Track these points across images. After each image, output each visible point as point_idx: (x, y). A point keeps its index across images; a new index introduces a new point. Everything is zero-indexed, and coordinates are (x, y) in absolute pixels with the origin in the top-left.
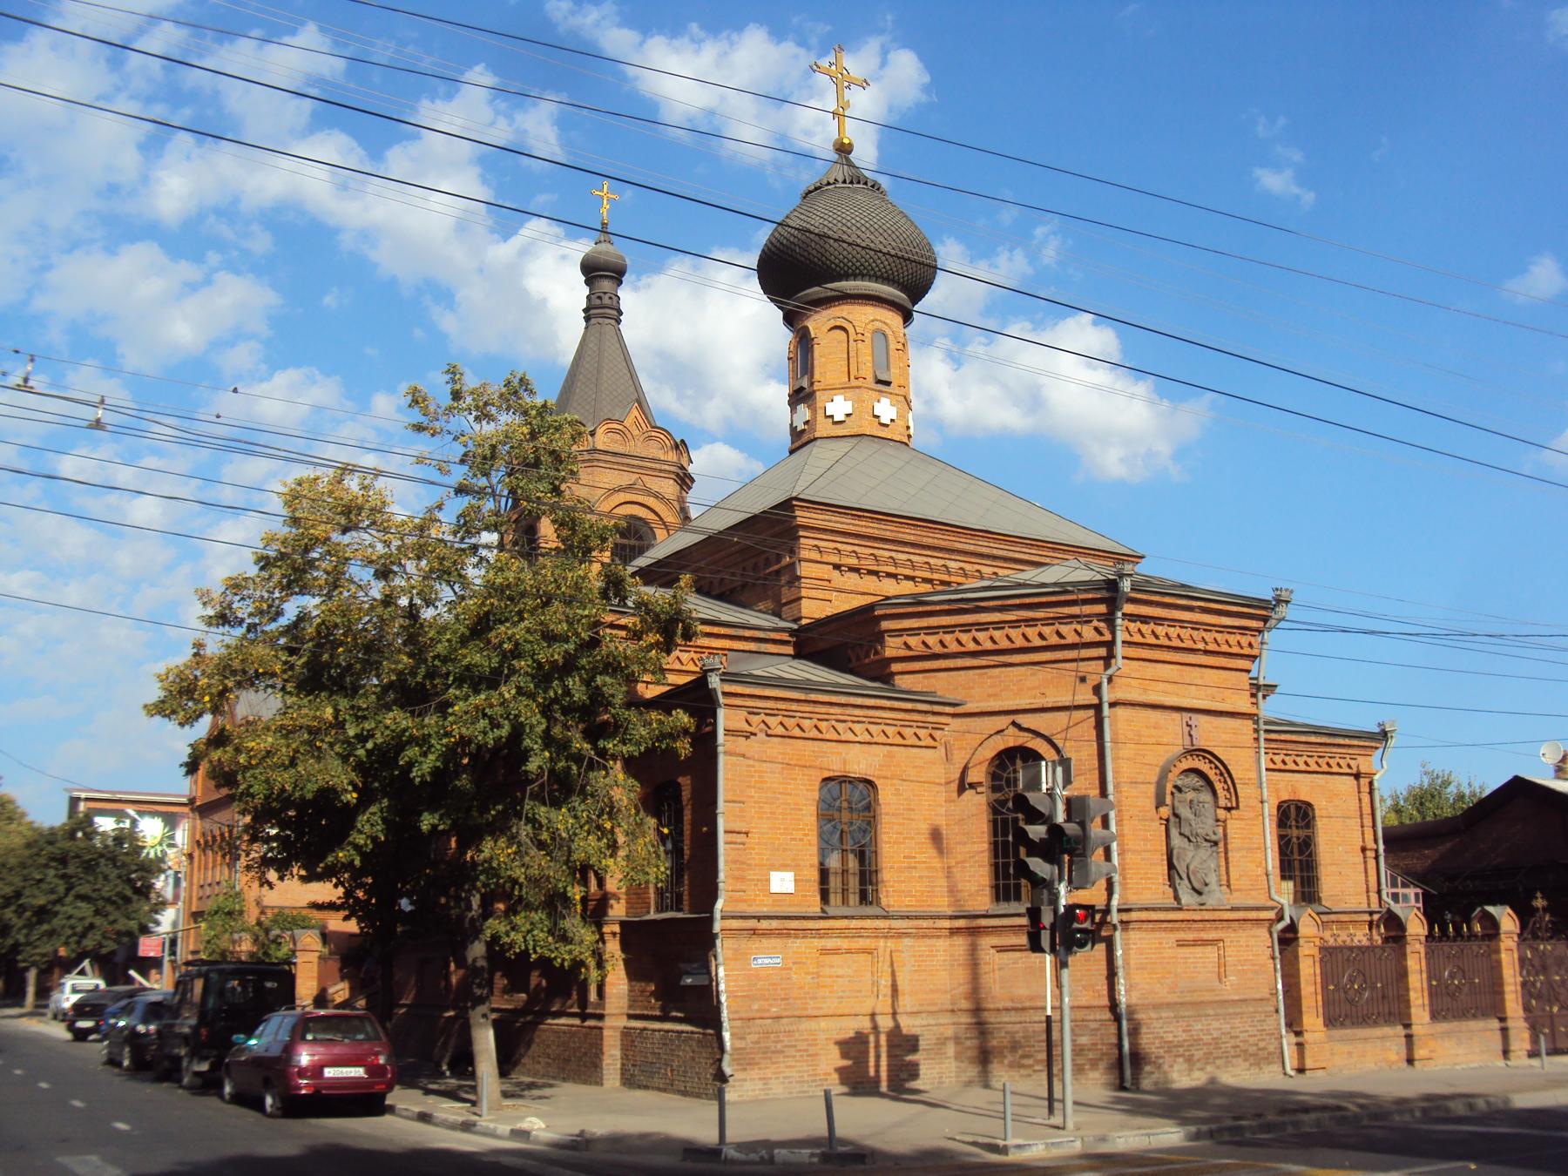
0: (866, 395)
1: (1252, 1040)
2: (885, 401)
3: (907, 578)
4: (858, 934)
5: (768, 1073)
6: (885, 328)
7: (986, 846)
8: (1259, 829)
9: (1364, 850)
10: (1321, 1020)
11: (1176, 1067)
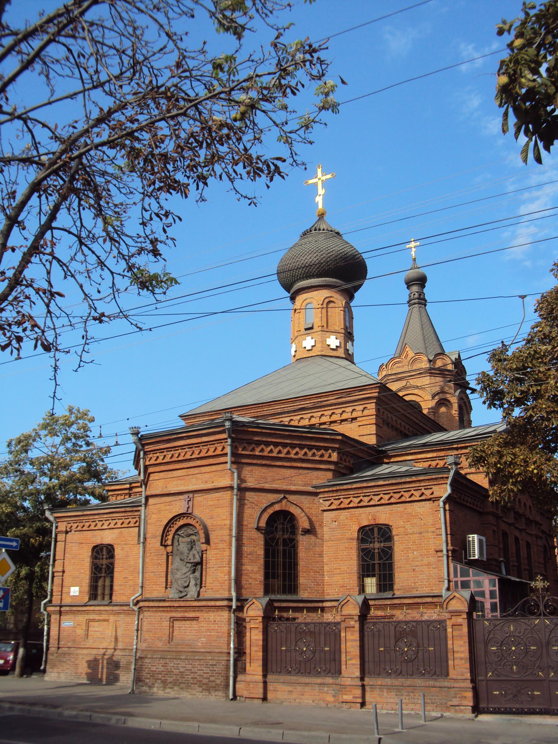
1: (205, 675)
4: (100, 612)
5: (60, 670)
8: (227, 553)
11: (156, 685)
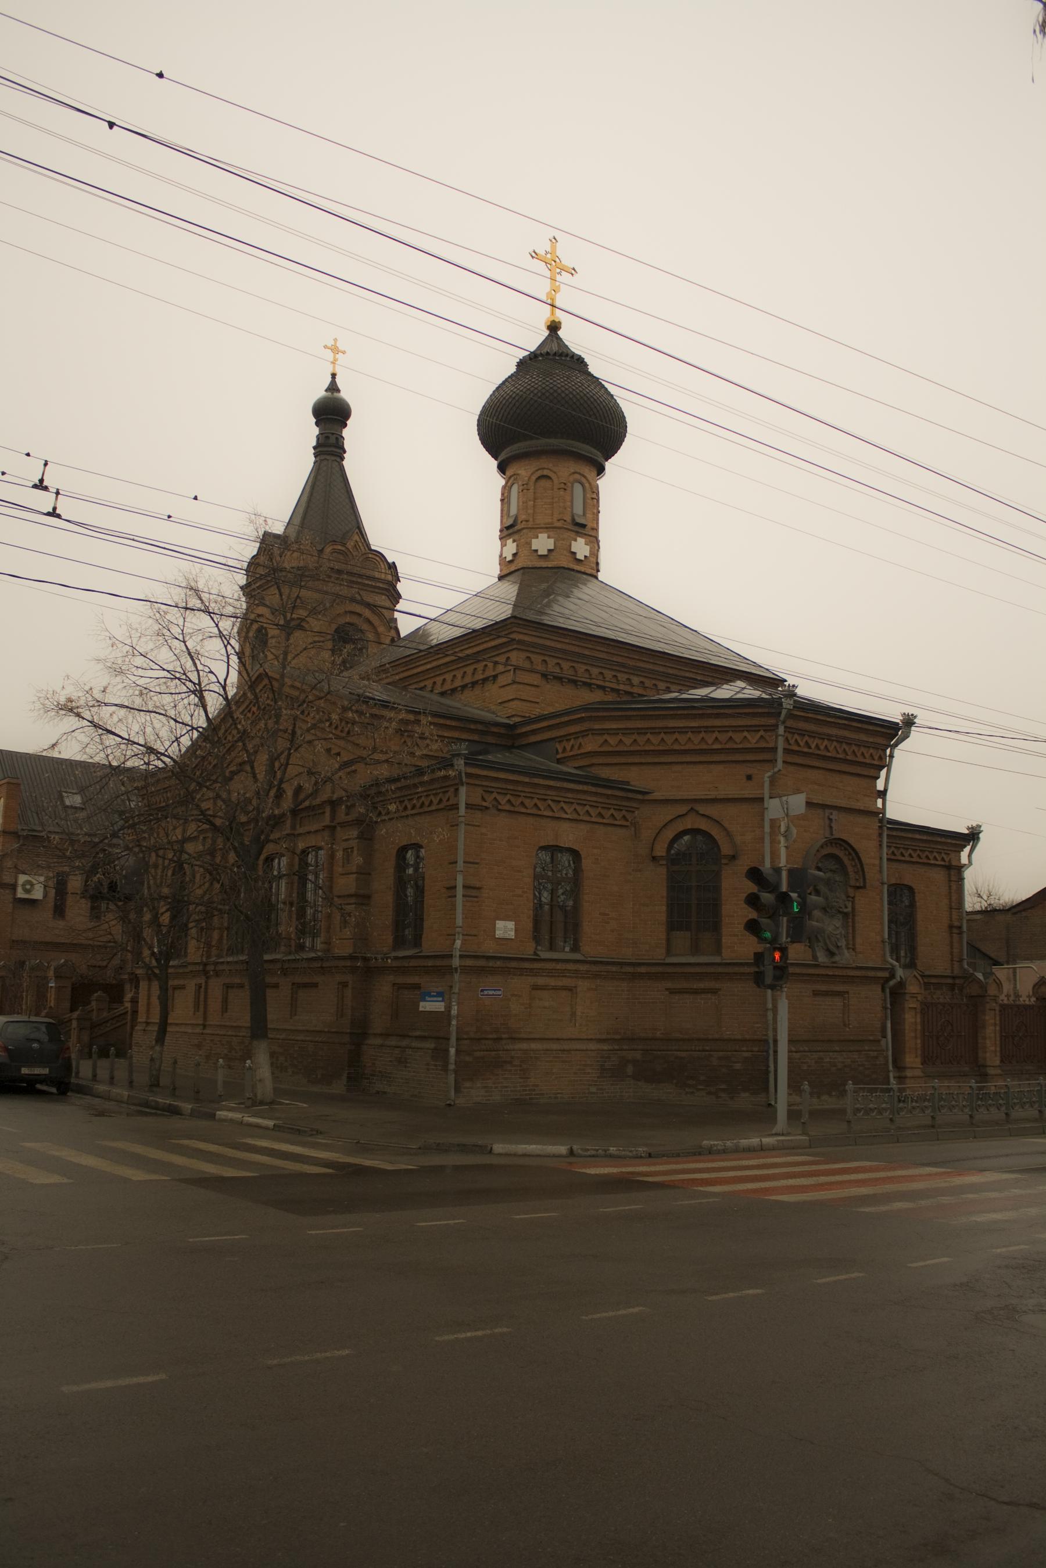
0: (567, 534)
2: (581, 541)
3: (613, 690)
6: (583, 480)
7: (664, 908)
9: (951, 927)
10: (919, 1060)
